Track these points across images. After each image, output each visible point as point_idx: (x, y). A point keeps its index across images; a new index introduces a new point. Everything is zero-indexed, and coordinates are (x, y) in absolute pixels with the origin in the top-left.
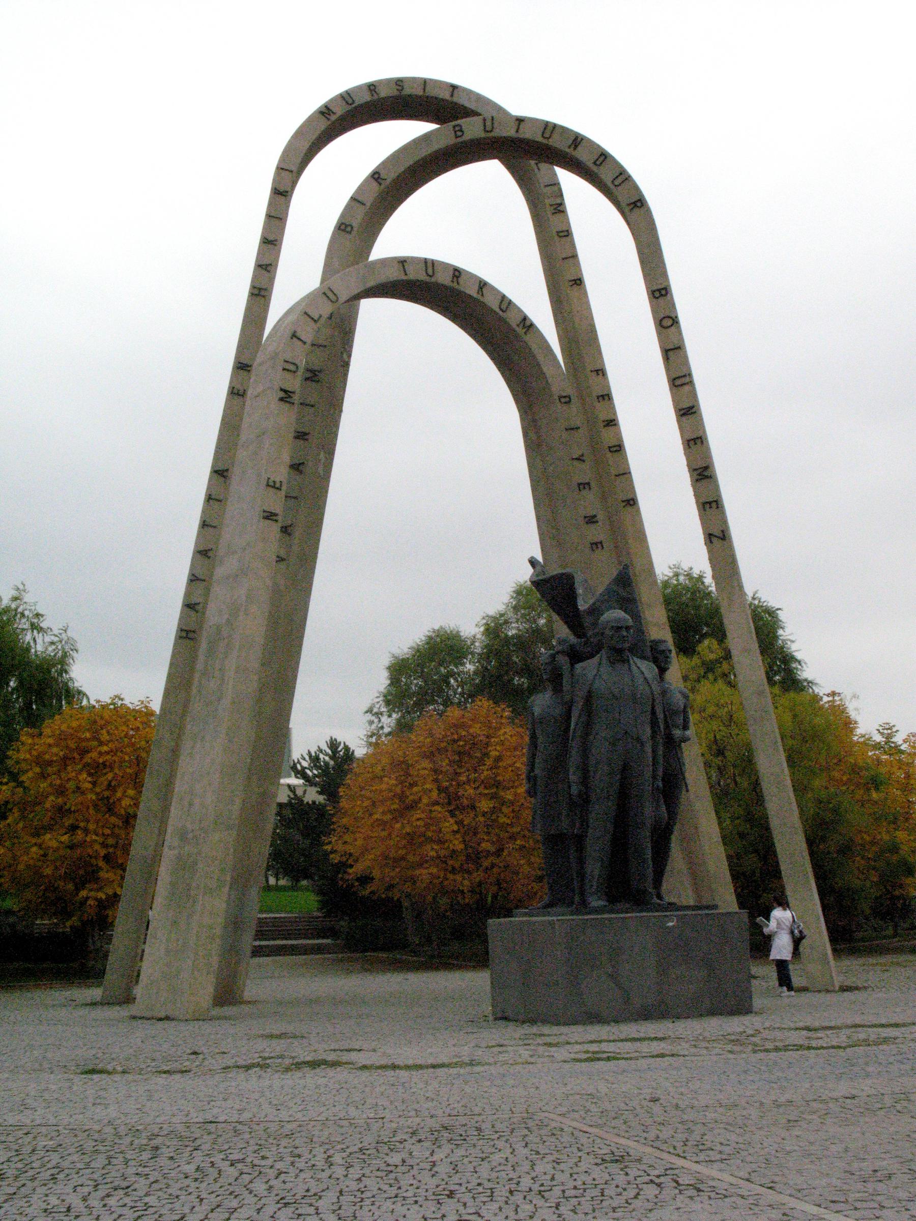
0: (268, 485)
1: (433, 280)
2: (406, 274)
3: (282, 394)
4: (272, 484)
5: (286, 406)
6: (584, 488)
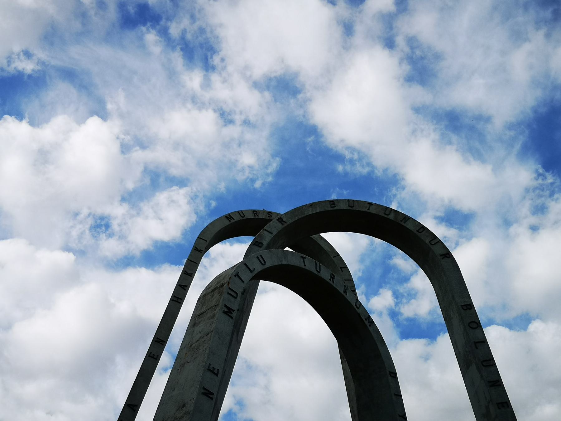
0: (209, 370)
1: (319, 274)
2: (305, 265)
3: (226, 310)
5: (227, 318)
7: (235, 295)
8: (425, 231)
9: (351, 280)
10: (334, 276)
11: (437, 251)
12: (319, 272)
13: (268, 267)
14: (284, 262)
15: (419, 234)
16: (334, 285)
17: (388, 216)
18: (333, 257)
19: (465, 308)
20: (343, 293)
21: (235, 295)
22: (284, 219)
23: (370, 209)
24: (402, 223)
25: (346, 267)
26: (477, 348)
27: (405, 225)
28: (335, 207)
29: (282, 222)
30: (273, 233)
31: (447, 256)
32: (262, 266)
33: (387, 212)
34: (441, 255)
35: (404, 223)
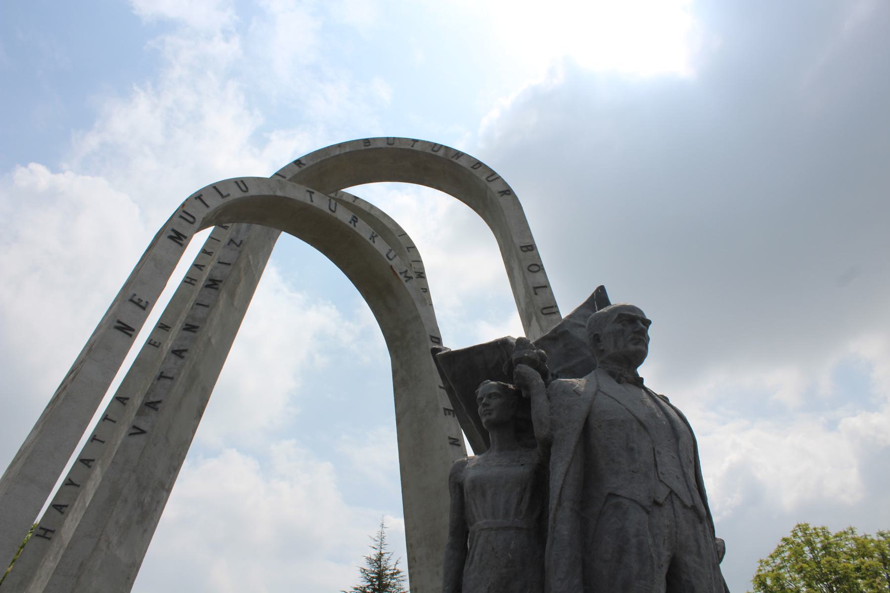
1: (334, 215)
3: (173, 234)
4: (136, 299)
6: (450, 414)
7: (191, 219)
8: (481, 168)
9: (419, 261)
10: (356, 218)
11: (495, 187)
12: (334, 212)
13: (252, 196)
14: (279, 193)
15: (473, 170)
16: (356, 229)
17: (437, 153)
18: (399, 236)
19: (524, 249)
20: (369, 240)
21: (191, 219)
22: (303, 162)
23: (414, 146)
24: (454, 160)
25: (414, 247)
26: (536, 294)
27: (456, 161)
28: (370, 145)
29: (301, 165)
30: (287, 177)
31: (508, 193)
32: (242, 192)
33: (435, 149)
34: (499, 192)
35: (456, 159)
